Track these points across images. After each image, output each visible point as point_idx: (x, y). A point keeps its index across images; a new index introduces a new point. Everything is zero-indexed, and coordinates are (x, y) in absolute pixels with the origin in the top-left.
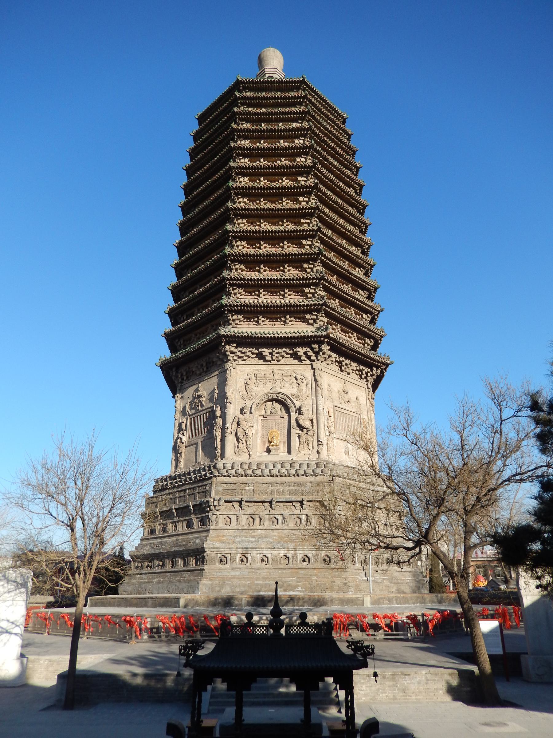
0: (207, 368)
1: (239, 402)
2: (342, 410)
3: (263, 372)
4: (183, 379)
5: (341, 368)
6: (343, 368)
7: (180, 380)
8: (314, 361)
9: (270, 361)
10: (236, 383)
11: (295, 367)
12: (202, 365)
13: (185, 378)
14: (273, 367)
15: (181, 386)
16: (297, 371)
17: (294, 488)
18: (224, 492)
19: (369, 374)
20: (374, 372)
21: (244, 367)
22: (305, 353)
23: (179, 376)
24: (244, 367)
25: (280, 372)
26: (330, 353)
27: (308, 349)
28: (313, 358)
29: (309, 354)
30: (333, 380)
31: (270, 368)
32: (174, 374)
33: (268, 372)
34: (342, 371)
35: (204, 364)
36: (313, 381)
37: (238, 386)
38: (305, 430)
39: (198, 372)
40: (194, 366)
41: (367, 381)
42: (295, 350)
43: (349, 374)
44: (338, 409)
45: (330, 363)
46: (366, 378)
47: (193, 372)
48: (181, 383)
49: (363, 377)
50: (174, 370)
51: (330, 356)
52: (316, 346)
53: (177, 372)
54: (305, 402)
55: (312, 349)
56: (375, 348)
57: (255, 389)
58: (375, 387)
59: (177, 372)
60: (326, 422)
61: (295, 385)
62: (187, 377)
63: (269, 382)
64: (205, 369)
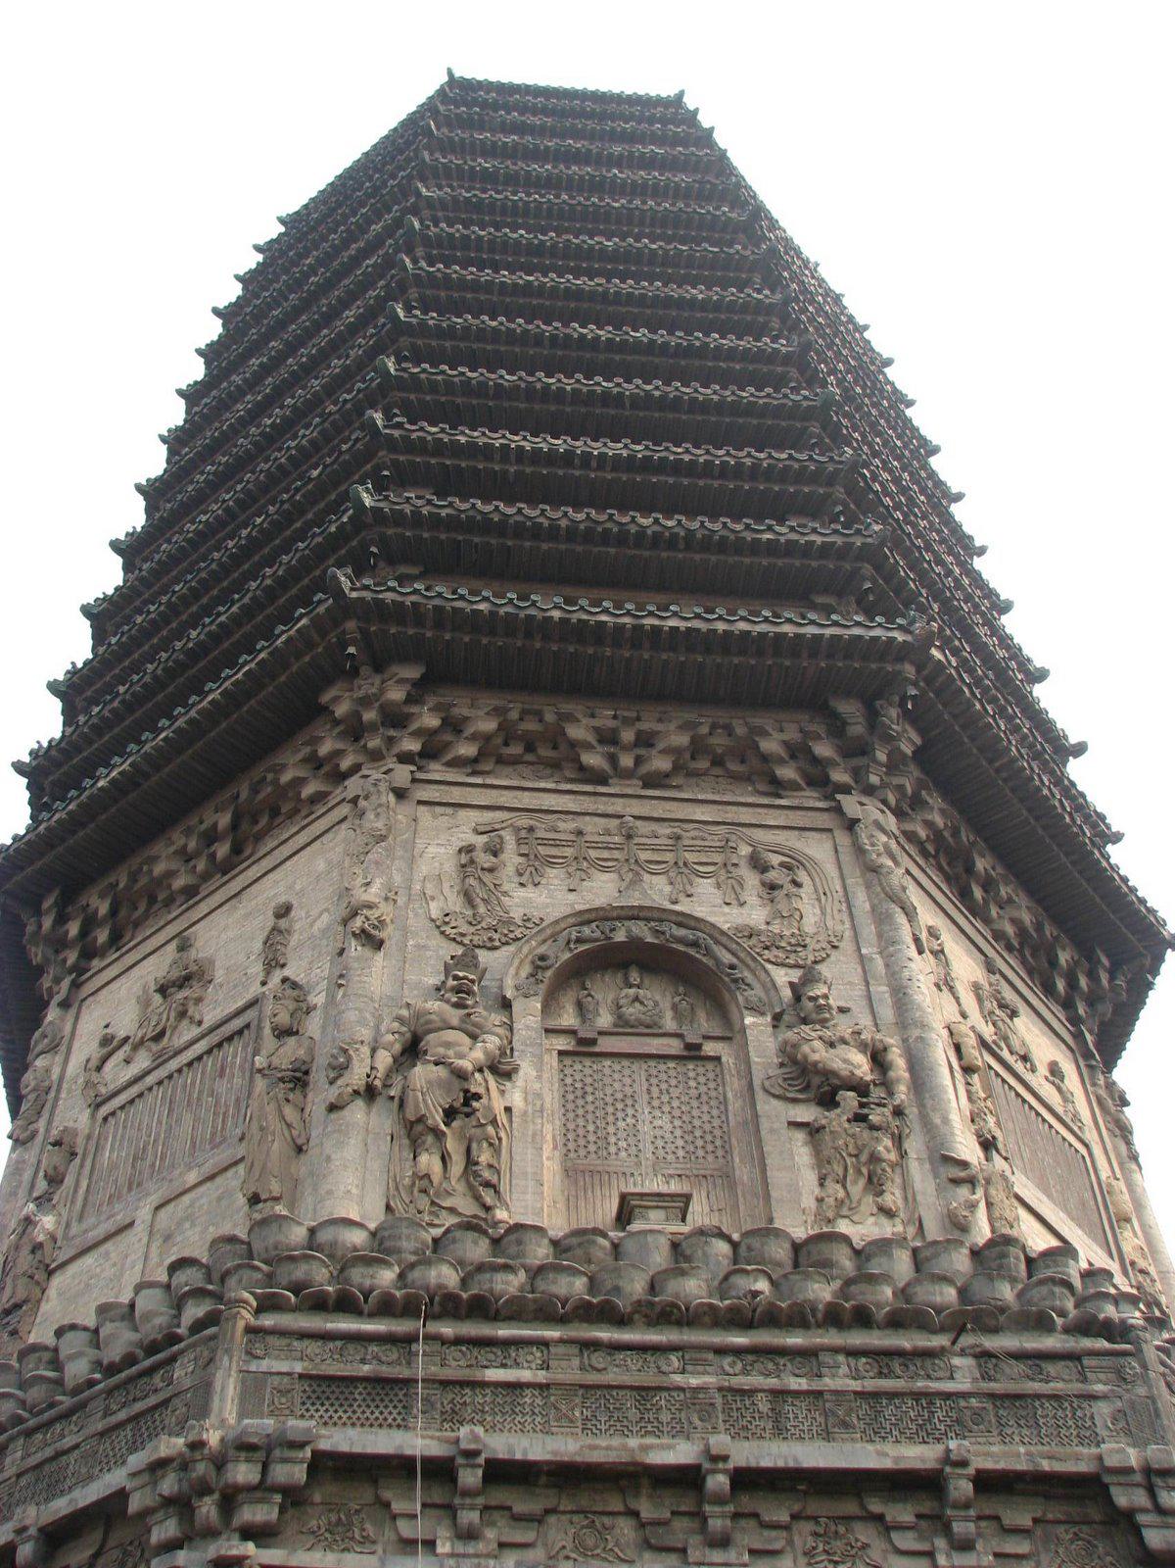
0: (237, 850)
3: (567, 825)
8: (846, 790)
9: (603, 780)
10: (412, 861)
11: (745, 815)
13: (102, 936)
14: (617, 806)
16: (760, 835)
20: (1104, 978)
21: (456, 795)
22: (797, 751)
23: (73, 929)
24: (456, 795)
25: (665, 830)
28: (839, 776)
29: (823, 750)
31: (601, 808)
32: (47, 923)
33: (591, 826)
36: (855, 881)
37: (418, 876)
38: (849, 1099)
39: (179, 883)
40: (162, 860)
42: (740, 730)
43: (998, 935)
48: (80, 970)
52: (849, 709)
53: (62, 919)
55: (837, 728)
57: (521, 893)
59: (62, 919)
63: (605, 870)
64: (222, 850)
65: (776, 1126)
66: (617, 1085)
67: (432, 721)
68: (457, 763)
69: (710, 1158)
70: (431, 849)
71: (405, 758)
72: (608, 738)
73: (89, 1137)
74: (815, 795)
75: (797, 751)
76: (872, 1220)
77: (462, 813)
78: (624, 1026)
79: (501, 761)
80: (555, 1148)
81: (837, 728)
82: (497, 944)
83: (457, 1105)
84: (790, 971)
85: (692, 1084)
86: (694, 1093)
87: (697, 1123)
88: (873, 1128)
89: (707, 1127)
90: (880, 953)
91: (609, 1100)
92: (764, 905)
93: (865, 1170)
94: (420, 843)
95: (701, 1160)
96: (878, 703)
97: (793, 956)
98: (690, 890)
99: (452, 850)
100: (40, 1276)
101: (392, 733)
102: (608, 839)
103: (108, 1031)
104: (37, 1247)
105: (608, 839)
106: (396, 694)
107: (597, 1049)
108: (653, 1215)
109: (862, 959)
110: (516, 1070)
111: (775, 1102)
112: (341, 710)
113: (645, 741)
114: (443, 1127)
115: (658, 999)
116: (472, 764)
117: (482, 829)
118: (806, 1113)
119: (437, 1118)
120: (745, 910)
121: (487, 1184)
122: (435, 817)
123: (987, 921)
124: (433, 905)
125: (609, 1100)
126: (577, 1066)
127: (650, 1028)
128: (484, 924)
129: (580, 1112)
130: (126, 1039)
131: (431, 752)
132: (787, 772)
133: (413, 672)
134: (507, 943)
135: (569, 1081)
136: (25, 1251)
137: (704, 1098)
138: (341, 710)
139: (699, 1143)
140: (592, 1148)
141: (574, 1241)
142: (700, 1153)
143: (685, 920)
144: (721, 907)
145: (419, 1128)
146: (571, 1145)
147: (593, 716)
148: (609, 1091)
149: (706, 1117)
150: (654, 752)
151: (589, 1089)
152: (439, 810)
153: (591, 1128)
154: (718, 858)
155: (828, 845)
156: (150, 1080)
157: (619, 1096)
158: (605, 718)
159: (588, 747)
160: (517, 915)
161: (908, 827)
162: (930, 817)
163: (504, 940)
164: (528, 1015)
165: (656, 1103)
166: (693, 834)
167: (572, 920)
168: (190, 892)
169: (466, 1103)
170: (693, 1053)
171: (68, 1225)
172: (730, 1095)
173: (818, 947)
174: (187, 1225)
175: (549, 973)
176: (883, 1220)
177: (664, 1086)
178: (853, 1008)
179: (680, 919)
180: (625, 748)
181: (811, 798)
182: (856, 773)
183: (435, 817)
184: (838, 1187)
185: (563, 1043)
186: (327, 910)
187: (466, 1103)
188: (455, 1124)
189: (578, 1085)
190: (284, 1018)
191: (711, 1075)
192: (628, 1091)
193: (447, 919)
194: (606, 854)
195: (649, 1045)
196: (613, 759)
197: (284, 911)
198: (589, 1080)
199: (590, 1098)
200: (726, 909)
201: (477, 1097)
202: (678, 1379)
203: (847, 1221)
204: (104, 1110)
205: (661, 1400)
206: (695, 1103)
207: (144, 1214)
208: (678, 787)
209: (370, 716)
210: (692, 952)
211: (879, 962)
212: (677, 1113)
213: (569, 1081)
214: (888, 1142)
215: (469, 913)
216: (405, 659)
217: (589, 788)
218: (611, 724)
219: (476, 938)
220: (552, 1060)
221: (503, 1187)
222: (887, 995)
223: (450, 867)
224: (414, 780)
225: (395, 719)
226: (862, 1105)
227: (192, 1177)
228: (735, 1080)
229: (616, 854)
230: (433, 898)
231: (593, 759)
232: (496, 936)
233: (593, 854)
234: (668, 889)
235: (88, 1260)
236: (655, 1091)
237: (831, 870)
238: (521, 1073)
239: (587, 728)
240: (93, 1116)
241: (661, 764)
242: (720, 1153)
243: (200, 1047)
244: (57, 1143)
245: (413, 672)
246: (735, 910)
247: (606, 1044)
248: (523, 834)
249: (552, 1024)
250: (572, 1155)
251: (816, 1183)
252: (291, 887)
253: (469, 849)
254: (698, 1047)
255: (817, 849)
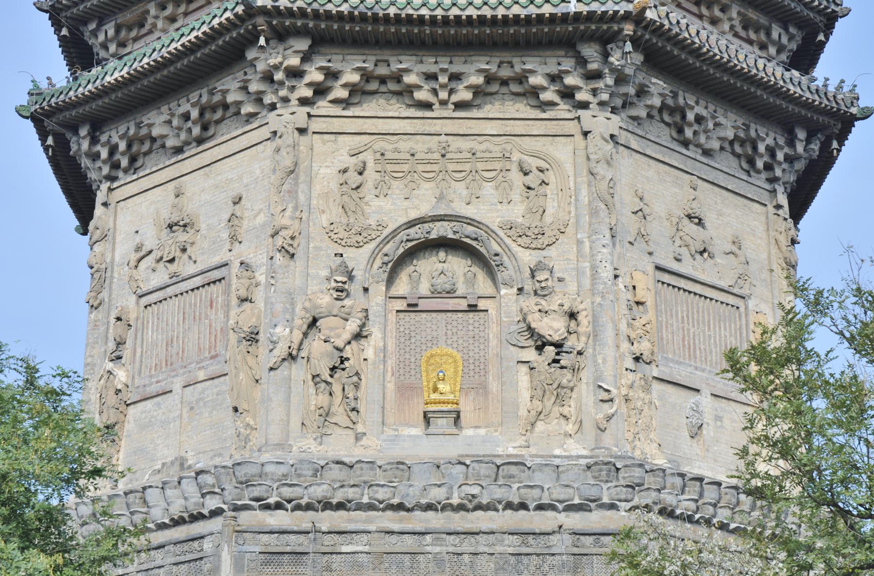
0: (205, 128)
1: (317, 248)
2: (682, 283)
3: (405, 145)
4: (116, 166)
5: (680, 131)
6: (689, 133)
7: (106, 170)
8: (585, 105)
11: (518, 127)
12: (186, 117)
13: (124, 163)
15: (110, 190)
17: (511, 550)
18: (266, 563)
19: (780, 156)
20: (800, 148)
21: (336, 125)
23: (104, 154)
24: (336, 125)
26: (641, 78)
27: (568, 64)
28: (580, 96)
29: (569, 80)
30: (651, 173)
32: (85, 145)
33: (420, 145)
34: (686, 144)
35: (195, 114)
36: (584, 178)
37: (314, 194)
38: (550, 350)
39: (170, 143)
41: (772, 180)
43: (707, 153)
44: (666, 278)
45: (643, 113)
46: (768, 167)
47: (153, 140)
49: (760, 164)
50: (84, 131)
51: (642, 92)
52: (590, 51)
54: (552, 252)
55: (582, 62)
56: (805, 58)
57: (376, 203)
58: (800, 201)
59: (94, 141)
60: (623, 326)
61: (517, 193)
62: (133, 160)
63: (429, 180)
64: (196, 131)
65: (511, 364)
66: (428, 330)
67: (319, 77)
68: (335, 101)
69: (477, 377)
70: (322, 171)
71: (304, 102)
72: (431, 77)
73: (137, 319)
74: (567, 107)
75: (554, 78)
76: (556, 421)
77: (341, 138)
78: (436, 293)
79: (365, 93)
80: (393, 375)
81: (582, 62)
82: (361, 244)
83: (337, 365)
84: (533, 252)
85: (471, 328)
86: (471, 333)
87: (471, 354)
88: (562, 368)
89: (477, 356)
90: (589, 237)
91: (423, 340)
92: (522, 202)
93: (555, 393)
94: (315, 168)
95: (472, 378)
96: (609, 46)
97: (535, 242)
98: (479, 194)
99: (334, 171)
100: (122, 407)
101: (293, 82)
102: (430, 156)
103: (138, 239)
104: (118, 391)
105: (430, 156)
106: (294, 61)
107: (419, 309)
108: (441, 422)
109: (579, 242)
110: (370, 335)
111: (512, 348)
112: (261, 66)
113: (456, 77)
114: (329, 379)
115: (457, 266)
116: (345, 103)
117: (353, 152)
118: (531, 355)
119: (326, 375)
120: (511, 206)
121: (353, 409)
122: (324, 143)
123: (698, 146)
124: (324, 217)
125: (423, 340)
126: (407, 319)
127: (450, 293)
128: (353, 231)
129: (407, 349)
130: (150, 252)
131: (320, 91)
132: (548, 96)
133: (303, 45)
134: (367, 242)
135: (402, 329)
136: (112, 392)
137: (477, 337)
138: (261, 66)
139: (472, 367)
140: (413, 372)
141: (389, 467)
142: (472, 374)
143: (471, 222)
144: (491, 209)
145: (318, 379)
146: (402, 371)
147: (421, 62)
148: (424, 334)
149: (476, 350)
150: (461, 87)
151: (413, 334)
152: (326, 137)
153: (413, 360)
154: (498, 166)
155: (570, 148)
156: (170, 291)
157: (429, 338)
158: (430, 64)
159: (419, 87)
160: (372, 222)
161: (634, 112)
162: (649, 102)
163: (365, 240)
164: (379, 290)
165: (449, 342)
166: (483, 147)
167: (404, 227)
168: (179, 150)
169: (342, 362)
170: (474, 309)
171: (133, 378)
172: (491, 336)
173: (552, 234)
174: (201, 403)
175: (390, 265)
176: (563, 421)
177: (455, 330)
178: (568, 279)
179: (468, 221)
180: (443, 86)
181: (563, 109)
182: (594, 92)
183: (324, 143)
184: (539, 403)
185: (401, 305)
186: (261, 210)
187: (342, 362)
188: (336, 376)
189: (407, 332)
190: (243, 293)
191: (482, 322)
192: (435, 333)
193: (332, 227)
194: (429, 168)
195: (448, 304)
196: (435, 92)
197: (237, 201)
198: (413, 328)
199: (413, 340)
200: (499, 206)
201: (348, 359)
202: (428, 549)
203: (542, 422)
204: (145, 301)
205: (421, 558)
206: (471, 341)
207: (177, 387)
208: (479, 106)
209: (279, 76)
210: (474, 243)
211: (587, 244)
212: (460, 348)
213: (402, 329)
214: (569, 376)
215: (344, 220)
216: (299, 33)
217: (420, 114)
218: (433, 69)
219: (349, 241)
220: (392, 317)
221: (362, 410)
222: (588, 269)
223: (334, 185)
224: (309, 116)
225: (295, 74)
226: (558, 354)
227: (201, 375)
228: (495, 325)
229: (435, 168)
230: (323, 212)
231: (421, 95)
232: (360, 238)
233: (421, 168)
234: (465, 192)
235: (149, 404)
236: (449, 333)
237: (569, 169)
238: (373, 336)
239: (418, 74)
240: (137, 303)
241: (465, 95)
242: (482, 373)
243: (198, 281)
244: (119, 319)
245: (303, 45)
246: (505, 207)
247: (423, 304)
248: (378, 156)
249: (394, 292)
250: (402, 378)
251: (529, 399)
252: (240, 178)
253: (345, 171)
254: (476, 306)
255: (563, 152)
